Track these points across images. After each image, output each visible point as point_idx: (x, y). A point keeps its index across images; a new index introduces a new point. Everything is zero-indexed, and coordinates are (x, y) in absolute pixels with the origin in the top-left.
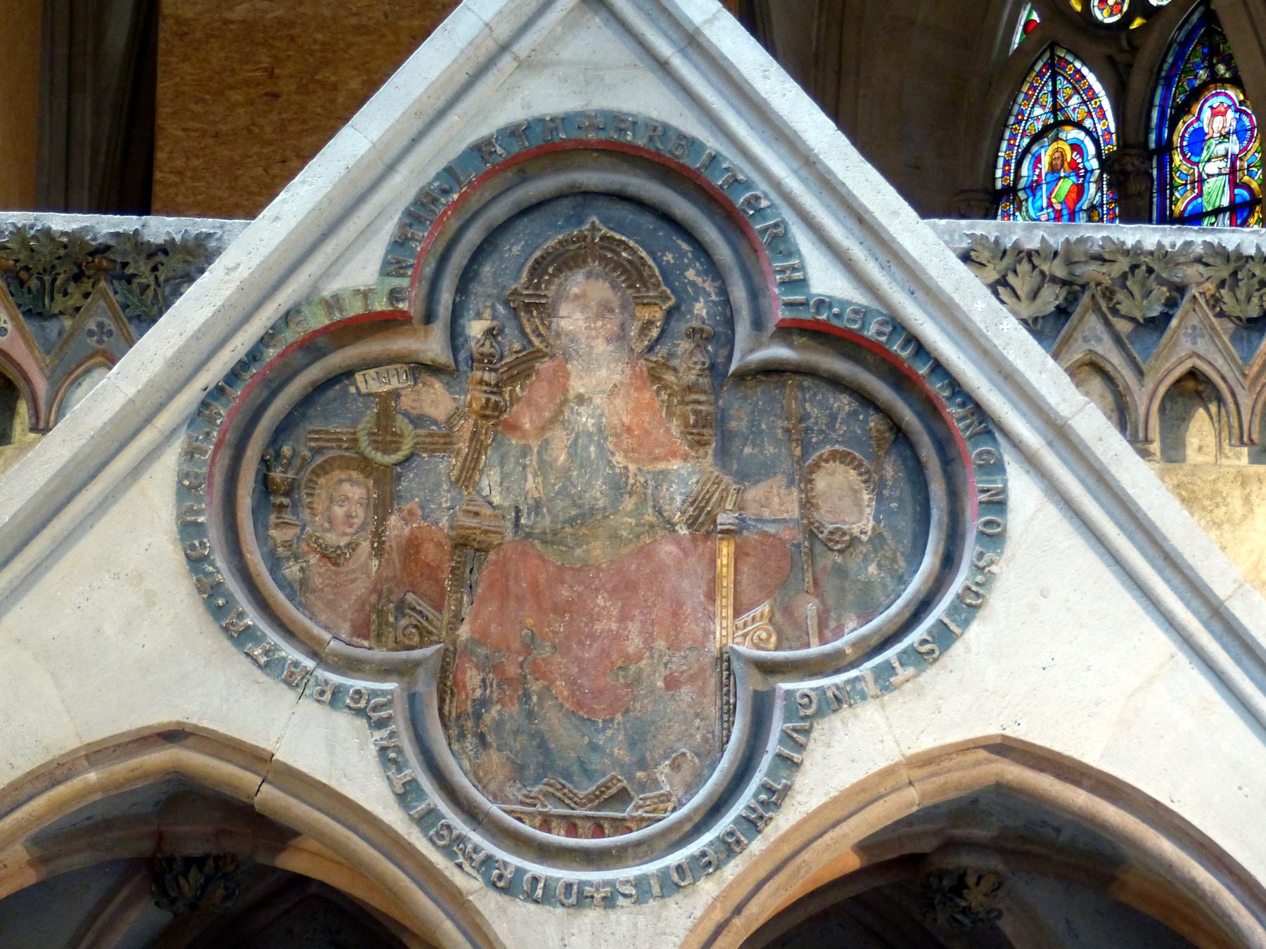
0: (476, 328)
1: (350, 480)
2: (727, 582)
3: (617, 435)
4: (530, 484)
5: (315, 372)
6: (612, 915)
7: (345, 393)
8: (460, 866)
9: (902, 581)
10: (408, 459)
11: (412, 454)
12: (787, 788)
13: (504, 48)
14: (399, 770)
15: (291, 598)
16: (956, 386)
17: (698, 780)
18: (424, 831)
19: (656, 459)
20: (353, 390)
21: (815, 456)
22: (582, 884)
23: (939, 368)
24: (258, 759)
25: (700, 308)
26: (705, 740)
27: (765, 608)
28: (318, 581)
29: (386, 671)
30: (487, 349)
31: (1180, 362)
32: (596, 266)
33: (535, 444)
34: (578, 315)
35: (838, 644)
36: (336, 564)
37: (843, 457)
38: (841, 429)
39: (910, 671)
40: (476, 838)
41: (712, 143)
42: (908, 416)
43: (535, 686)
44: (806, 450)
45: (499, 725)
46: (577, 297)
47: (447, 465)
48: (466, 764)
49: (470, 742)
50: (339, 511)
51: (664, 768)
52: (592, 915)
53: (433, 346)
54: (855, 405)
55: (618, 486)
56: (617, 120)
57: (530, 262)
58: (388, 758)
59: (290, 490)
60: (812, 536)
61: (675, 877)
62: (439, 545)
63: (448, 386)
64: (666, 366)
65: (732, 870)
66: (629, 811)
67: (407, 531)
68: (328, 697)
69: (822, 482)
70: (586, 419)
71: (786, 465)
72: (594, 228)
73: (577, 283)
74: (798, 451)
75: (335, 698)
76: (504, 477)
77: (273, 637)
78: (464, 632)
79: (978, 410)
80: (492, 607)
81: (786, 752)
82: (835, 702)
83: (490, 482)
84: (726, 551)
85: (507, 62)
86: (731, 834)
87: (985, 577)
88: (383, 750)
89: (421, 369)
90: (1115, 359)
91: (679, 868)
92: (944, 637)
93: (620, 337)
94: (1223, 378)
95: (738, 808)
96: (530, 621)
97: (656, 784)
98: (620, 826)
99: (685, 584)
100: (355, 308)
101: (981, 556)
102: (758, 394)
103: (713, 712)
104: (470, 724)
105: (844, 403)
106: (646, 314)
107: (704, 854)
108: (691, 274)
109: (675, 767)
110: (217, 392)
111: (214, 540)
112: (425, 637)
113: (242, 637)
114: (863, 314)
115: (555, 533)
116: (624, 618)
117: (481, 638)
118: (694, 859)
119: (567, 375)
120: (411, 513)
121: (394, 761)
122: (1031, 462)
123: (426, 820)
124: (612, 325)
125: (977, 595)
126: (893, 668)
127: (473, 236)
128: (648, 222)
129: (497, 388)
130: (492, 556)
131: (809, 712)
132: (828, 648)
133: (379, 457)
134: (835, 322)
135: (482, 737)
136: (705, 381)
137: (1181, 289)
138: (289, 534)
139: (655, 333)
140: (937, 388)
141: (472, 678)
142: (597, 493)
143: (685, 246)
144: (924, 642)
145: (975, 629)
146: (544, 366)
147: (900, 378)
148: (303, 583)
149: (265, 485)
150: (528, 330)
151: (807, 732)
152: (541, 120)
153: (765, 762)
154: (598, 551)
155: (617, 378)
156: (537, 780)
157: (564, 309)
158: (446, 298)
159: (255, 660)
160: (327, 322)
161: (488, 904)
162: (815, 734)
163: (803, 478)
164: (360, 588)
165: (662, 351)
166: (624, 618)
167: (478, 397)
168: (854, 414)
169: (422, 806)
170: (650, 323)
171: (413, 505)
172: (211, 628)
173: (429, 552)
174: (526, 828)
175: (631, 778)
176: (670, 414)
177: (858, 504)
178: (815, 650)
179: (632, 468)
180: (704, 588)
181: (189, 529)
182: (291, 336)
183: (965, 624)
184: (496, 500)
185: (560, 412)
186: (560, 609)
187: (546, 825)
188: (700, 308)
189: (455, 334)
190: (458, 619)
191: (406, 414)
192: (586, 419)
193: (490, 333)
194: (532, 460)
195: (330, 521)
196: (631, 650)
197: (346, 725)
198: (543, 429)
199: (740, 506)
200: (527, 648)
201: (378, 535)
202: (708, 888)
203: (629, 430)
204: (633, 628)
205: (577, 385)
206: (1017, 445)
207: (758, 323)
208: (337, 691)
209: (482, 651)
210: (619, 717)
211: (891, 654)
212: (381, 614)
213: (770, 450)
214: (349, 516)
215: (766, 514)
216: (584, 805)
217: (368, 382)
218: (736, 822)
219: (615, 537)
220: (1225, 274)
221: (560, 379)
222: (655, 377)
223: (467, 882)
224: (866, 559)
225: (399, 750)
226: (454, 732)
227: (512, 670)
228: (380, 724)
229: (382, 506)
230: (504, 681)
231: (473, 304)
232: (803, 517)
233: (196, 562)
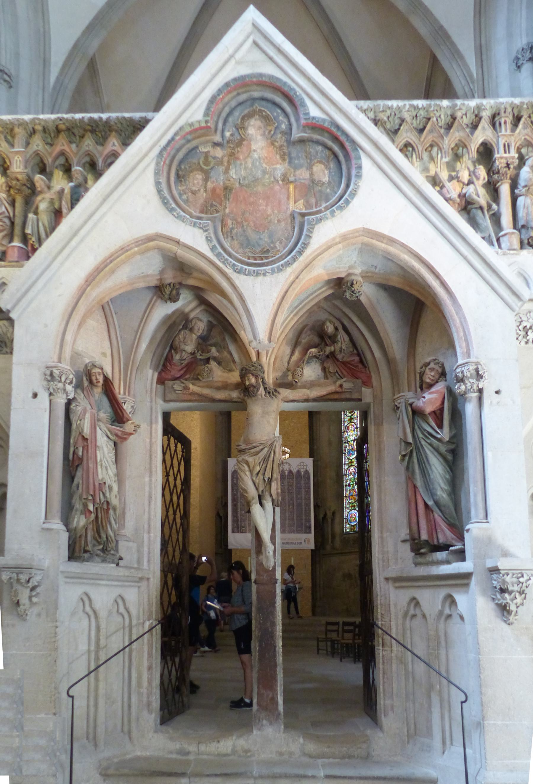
0: (227, 134)
1: (198, 174)
2: (292, 195)
3: (264, 159)
4: (242, 173)
6: (265, 278)
7: (196, 152)
8: (227, 266)
9: (336, 193)
10: (212, 169)
11: (213, 167)
12: (309, 243)
13: (232, 56)
14: (211, 242)
15: (185, 203)
17: (286, 246)
18: (218, 258)
19: (273, 165)
20: (198, 151)
21: (313, 162)
22: (257, 270)
25: (283, 126)
26: (288, 236)
27: (302, 201)
28: (191, 200)
30: (231, 138)
31: (403, 139)
32: (257, 117)
33: (243, 163)
34: (253, 129)
35: (320, 208)
36: (195, 195)
37: (320, 162)
38: (319, 155)
39: (339, 212)
40: (230, 259)
43: (245, 224)
44: (311, 160)
45: (236, 234)
46: (253, 125)
47: (221, 169)
48: (229, 244)
49: (229, 238)
50: (195, 182)
52: (260, 278)
54: (323, 149)
55: (264, 172)
56: (261, 75)
57: (241, 117)
58: (208, 239)
59: (184, 176)
60: (313, 182)
61: (281, 267)
62: (220, 189)
63: (222, 149)
64: (276, 141)
65: (295, 265)
66: (270, 254)
67: (212, 186)
68: (193, 224)
69: (315, 169)
70: (256, 155)
71: (306, 165)
72: (256, 107)
73: (253, 122)
74: (309, 161)
75: (195, 225)
76: (236, 171)
77: (179, 210)
78: (227, 211)
80: (234, 204)
81: (308, 234)
82: (320, 220)
83: (232, 173)
84: (291, 187)
85: (233, 62)
86: (295, 256)
87: (357, 187)
88: (207, 237)
91: (282, 265)
92: (347, 202)
93: (264, 134)
94: (414, 143)
95: (297, 249)
96: (243, 207)
97: (276, 247)
98: (267, 258)
99: (282, 196)
100: (197, 126)
101: (356, 181)
102: (298, 147)
103: (290, 228)
104: (229, 234)
105: (320, 148)
106: (270, 128)
107: (288, 261)
108: (281, 118)
109: (281, 243)
112: (217, 212)
113: (171, 210)
115: (249, 185)
116: (266, 206)
117: (231, 212)
118: (286, 262)
119: (251, 145)
120: (213, 181)
121: (209, 240)
123: (218, 255)
124: (261, 132)
125: (355, 191)
126: (335, 211)
127: (227, 110)
128: (270, 105)
130: (234, 191)
131: (314, 223)
132: (318, 209)
133: (205, 167)
134: (317, 123)
135: (232, 237)
136: (285, 144)
138: (184, 188)
139: (272, 132)
141: (230, 222)
142: (259, 174)
143: (279, 111)
144: (342, 204)
145: (355, 199)
146: (245, 143)
147: (335, 139)
148: (188, 200)
150: (241, 133)
151: (313, 228)
152: (242, 76)
153: (303, 237)
154: (260, 189)
155: (263, 145)
156: (247, 247)
157: (250, 128)
158: (220, 125)
159: (174, 216)
160: (190, 129)
161: (234, 276)
162: (315, 229)
163: (310, 168)
164: (201, 201)
165: (274, 137)
166: (266, 206)
168: (322, 151)
169: (217, 251)
170: (271, 130)
171: (214, 179)
174: (244, 259)
175: (270, 246)
176: (277, 153)
177: (324, 174)
178: (315, 210)
179: (268, 167)
180: (286, 196)
183: (352, 199)
184: (234, 177)
185: (249, 154)
187: (249, 259)
188: (283, 126)
190: (225, 207)
191: (212, 157)
192: (256, 155)
193: (232, 135)
194: (243, 166)
195: (194, 184)
196: (269, 214)
197: (197, 232)
198: (245, 158)
199: (295, 176)
200: (243, 214)
201: (205, 187)
202: (289, 270)
203: (266, 158)
204: (269, 208)
205: (253, 147)
209: (232, 215)
210: (266, 231)
211: (334, 208)
212: (206, 207)
213: (302, 161)
214: (198, 183)
215: (301, 177)
216: (258, 253)
218: (296, 252)
219: (264, 185)
220: (414, 114)
221: (249, 145)
222: (272, 144)
223: (229, 271)
224: (327, 188)
225: (211, 237)
226: (225, 236)
227: (239, 220)
228: (206, 231)
229: (206, 180)
230: (238, 223)
231: (227, 128)
232: (310, 177)
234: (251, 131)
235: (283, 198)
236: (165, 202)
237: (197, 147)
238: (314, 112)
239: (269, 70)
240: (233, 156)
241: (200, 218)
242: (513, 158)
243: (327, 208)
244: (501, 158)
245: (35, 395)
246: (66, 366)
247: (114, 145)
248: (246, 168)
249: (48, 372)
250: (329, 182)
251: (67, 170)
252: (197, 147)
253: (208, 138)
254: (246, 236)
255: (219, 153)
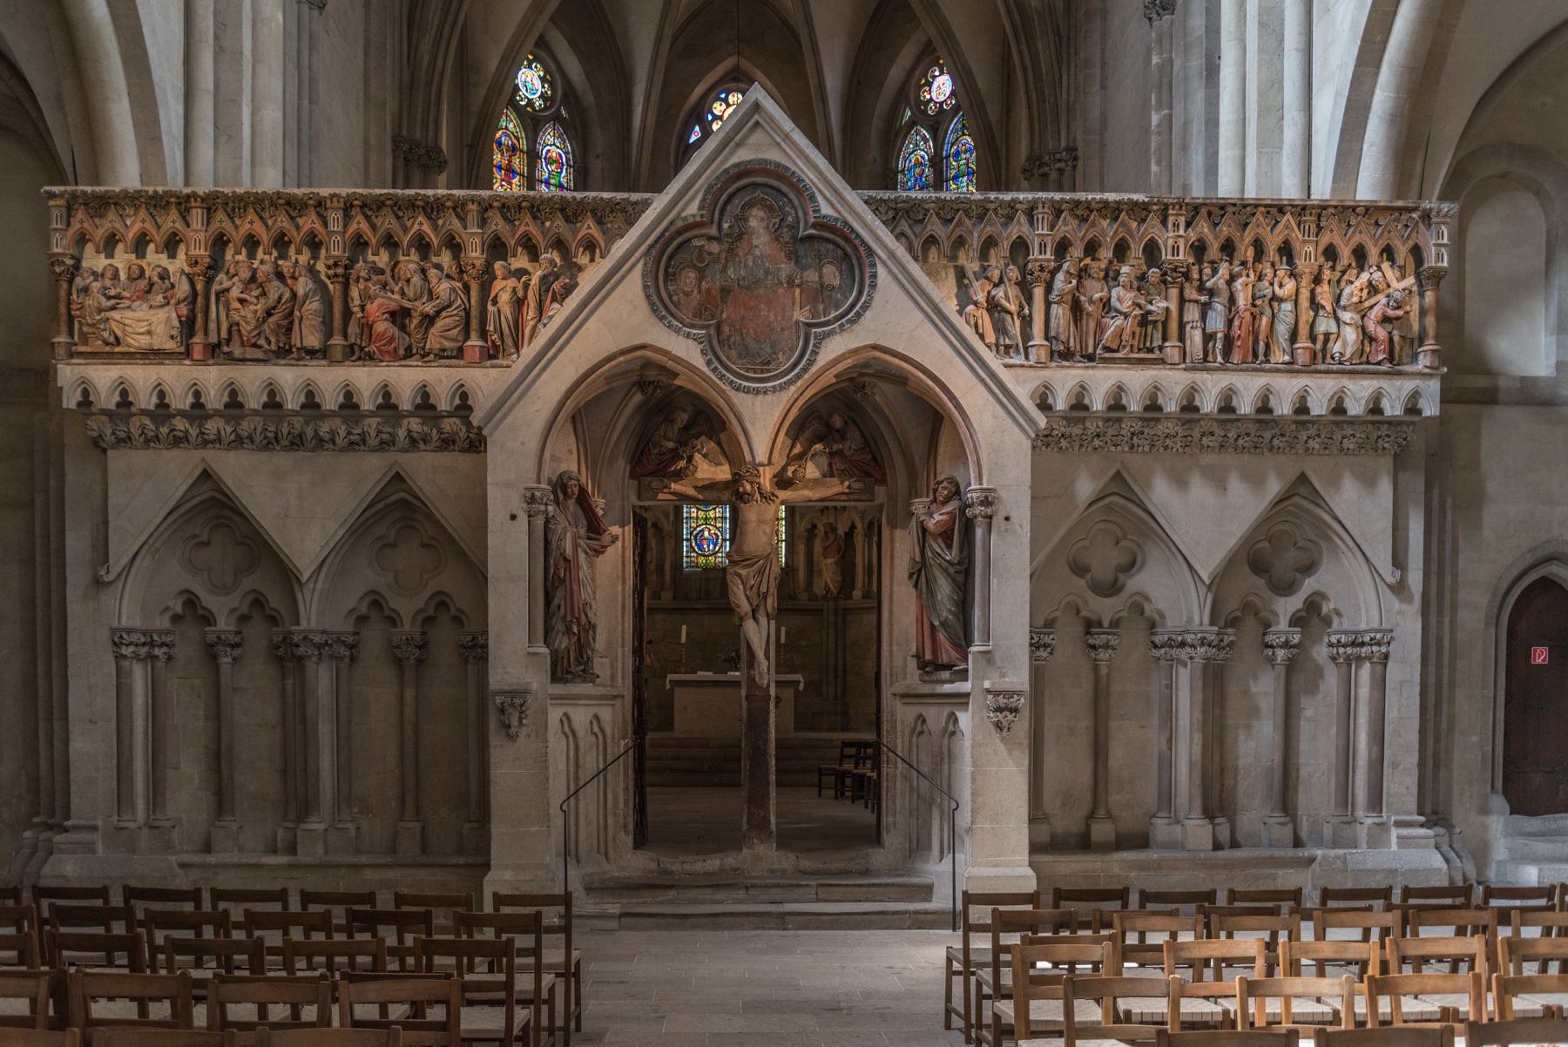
0: (725, 226)
5: (679, 240)
16: (863, 241)
17: (790, 357)
23: (858, 236)
24: (666, 353)
25: (790, 219)
29: (702, 328)
41: (793, 168)
42: (849, 250)
51: (781, 354)
53: (713, 231)
69: (825, 270)
70: (758, 253)
73: (755, 212)
75: (688, 336)
77: (670, 318)
78: (724, 316)
79: (869, 249)
83: (730, 271)
89: (710, 238)
90: (909, 232)
92: (859, 315)
93: (767, 228)
95: (801, 366)
98: (769, 371)
100: (691, 220)
105: (831, 247)
110: (652, 246)
111: (652, 290)
112: (713, 317)
113: (662, 318)
114: (836, 220)
117: (728, 318)
122: (884, 263)
124: (764, 224)
127: (724, 197)
129: (732, 244)
137: (928, 210)
140: (857, 242)
141: (726, 329)
142: (761, 274)
146: (746, 236)
147: (847, 239)
149: (666, 274)
154: (761, 291)
158: (716, 216)
161: (732, 393)
164: (695, 303)
167: (726, 246)
172: (652, 315)
173: (714, 292)
181: (645, 287)
182: (673, 229)
186: (751, 309)
187: (747, 371)
189: (720, 228)
190: (722, 312)
202: (793, 388)
205: (755, 242)
206: (880, 258)
207: (806, 223)
208: (689, 334)
217: (695, 243)
222: (777, 239)
229: (700, 279)
233: (648, 297)
234: (753, 223)
235: (788, 303)
236: (655, 311)
237: (689, 240)
238: (826, 210)
239: (774, 155)
240: (731, 251)
241: (692, 326)
242: (1048, 260)
243: (838, 318)
244: (1036, 260)
245: (513, 517)
246: (544, 486)
247: (589, 227)
248: (746, 267)
249: (529, 495)
250: (840, 286)
251: (534, 254)
252: (689, 240)
253: (703, 231)
254: (745, 345)
255: (715, 248)
